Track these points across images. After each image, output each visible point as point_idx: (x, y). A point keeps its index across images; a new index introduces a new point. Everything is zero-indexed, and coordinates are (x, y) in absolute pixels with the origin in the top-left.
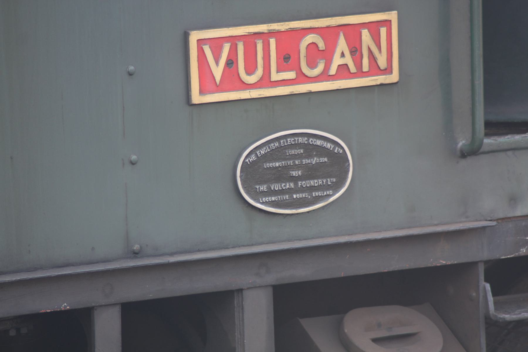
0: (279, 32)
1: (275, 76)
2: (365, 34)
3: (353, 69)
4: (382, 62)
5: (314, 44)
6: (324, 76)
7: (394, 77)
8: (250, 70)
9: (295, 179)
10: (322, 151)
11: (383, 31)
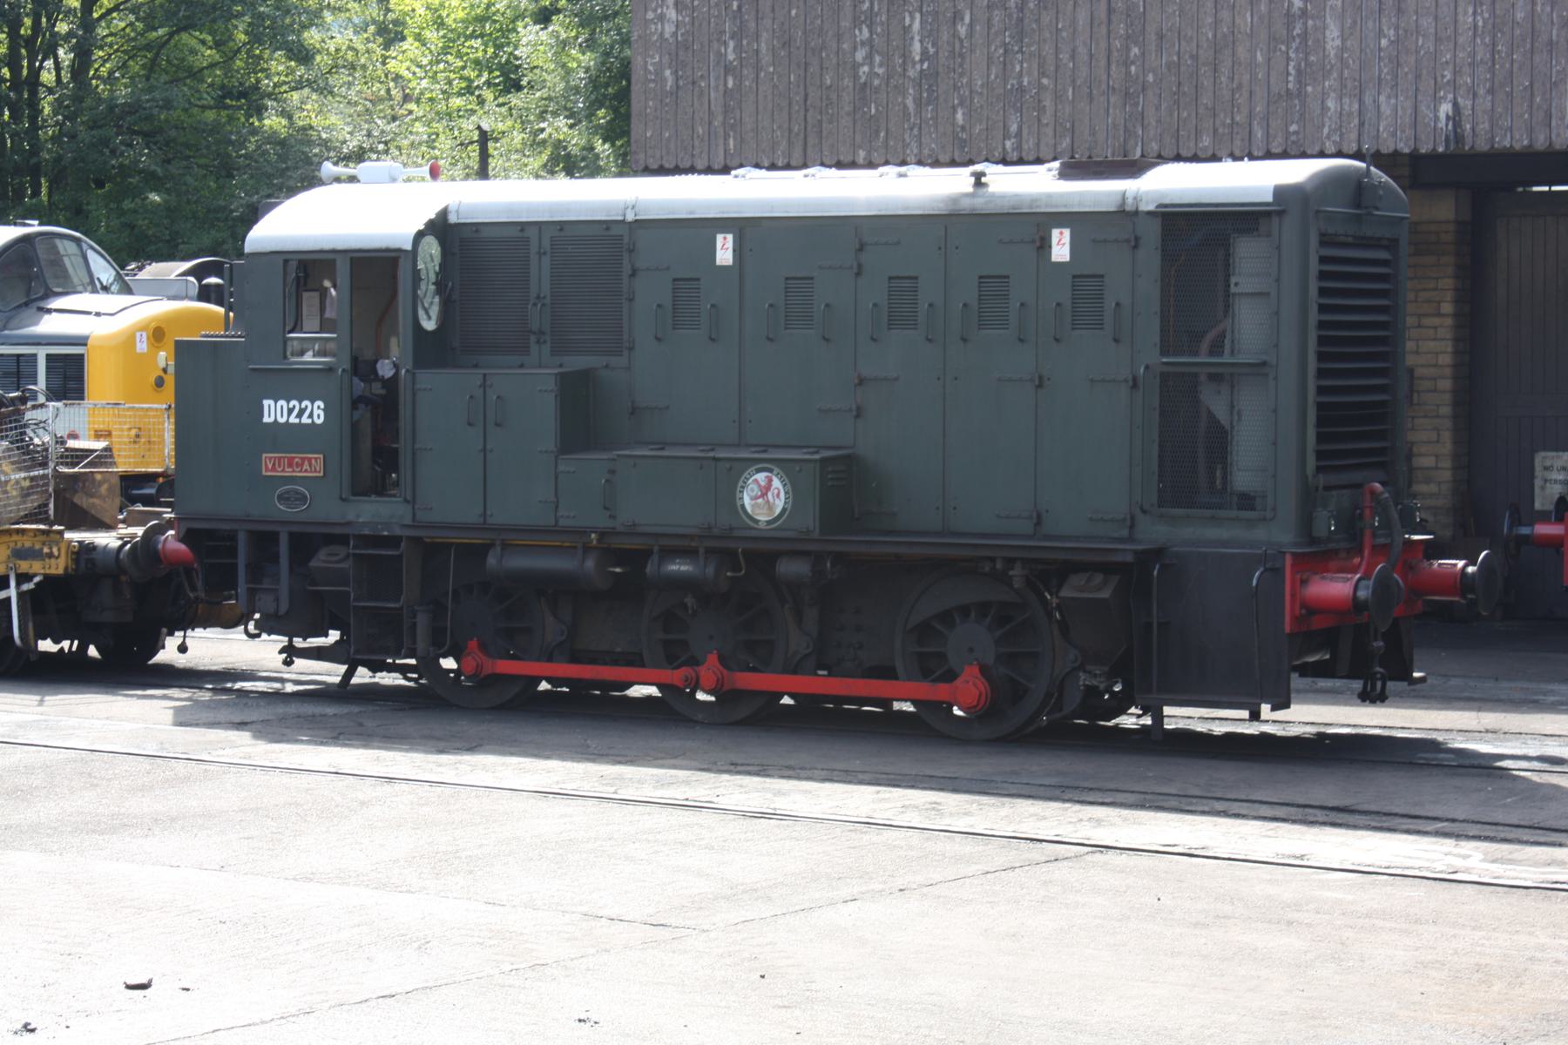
6: (301, 471)
8: (280, 466)
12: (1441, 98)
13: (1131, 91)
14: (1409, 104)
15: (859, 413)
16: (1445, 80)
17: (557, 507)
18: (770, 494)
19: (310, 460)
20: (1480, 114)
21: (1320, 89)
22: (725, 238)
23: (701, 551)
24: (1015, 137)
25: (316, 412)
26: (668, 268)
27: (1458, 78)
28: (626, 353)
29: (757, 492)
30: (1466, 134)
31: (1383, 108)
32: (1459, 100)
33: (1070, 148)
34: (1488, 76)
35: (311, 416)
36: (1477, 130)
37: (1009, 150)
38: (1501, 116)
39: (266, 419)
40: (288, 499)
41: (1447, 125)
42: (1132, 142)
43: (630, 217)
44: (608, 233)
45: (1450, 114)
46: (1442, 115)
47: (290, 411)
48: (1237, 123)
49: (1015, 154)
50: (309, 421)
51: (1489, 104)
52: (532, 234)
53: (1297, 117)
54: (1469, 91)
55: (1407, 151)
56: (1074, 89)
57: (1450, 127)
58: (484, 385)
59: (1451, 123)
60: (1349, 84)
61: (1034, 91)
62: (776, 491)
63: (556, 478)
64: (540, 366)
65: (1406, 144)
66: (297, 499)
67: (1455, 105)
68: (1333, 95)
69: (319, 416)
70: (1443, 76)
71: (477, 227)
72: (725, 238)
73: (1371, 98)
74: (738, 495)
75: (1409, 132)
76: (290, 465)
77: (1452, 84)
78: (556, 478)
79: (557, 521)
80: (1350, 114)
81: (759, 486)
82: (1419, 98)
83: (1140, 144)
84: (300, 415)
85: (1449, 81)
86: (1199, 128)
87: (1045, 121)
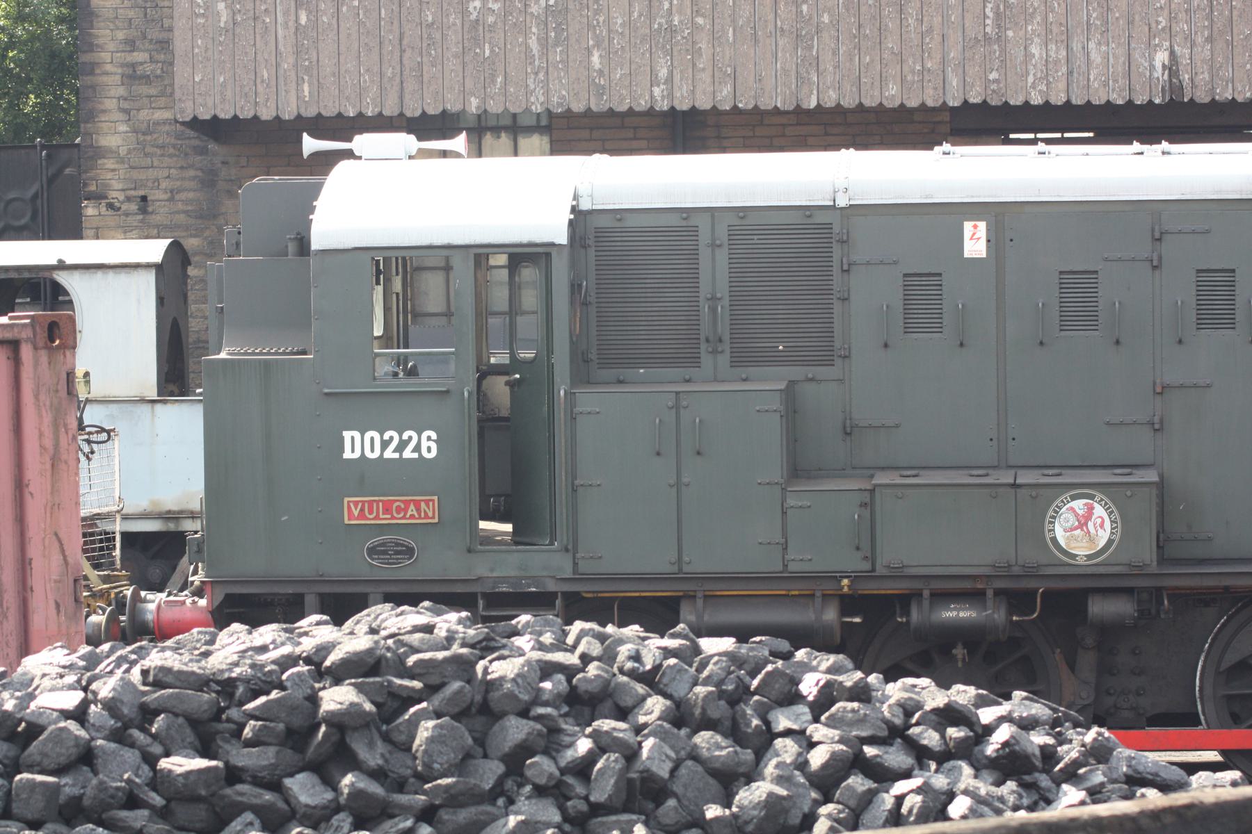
1: (381, 516)
3: (417, 516)
4: (430, 514)
5: (398, 507)
6: (404, 518)
7: (436, 520)
8: (371, 512)
10: (402, 545)
11: (431, 504)
12: (1156, 45)
13: (804, 33)
14: (1121, 52)
15: (1158, 428)
16: (1160, 27)
17: (785, 549)
18: (1090, 524)
20: (1199, 64)
21: (1022, 33)
22: (975, 227)
23: (990, 593)
24: (664, 84)
25: (428, 445)
26: (895, 263)
27: (1174, 25)
28: (838, 362)
29: (1073, 521)
30: (1184, 84)
31: (1093, 55)
32: (1176, 48)
33: (731, 96)
34: (1206, 24)
35: (417, 448)
36: (1197, 80)
37: (659, 99)
38: (1221, 67)
39: (348, 455)
40: (385, 553)
41: (1163, 74)
42: (805, 90)
43: (842, 202)
44: (744, 222)
45: (1166, 63)
46: (1158, 65)
47: (385, 445)
48: (929, 70)
49: (666, 102)
50: (416, 455)
51: (1209, 53)
52: (703, 223)
53: (997, 64)
54: (1186, 39)
55: (1120, 102)
56: (734, 30)
57: (1166, 77)
58: (677, 407)
59: (1167, 72)
60: (1055, 29)
61: (687, 32)
62: (1099, 520)
64: (716, 380)
65: (1119, 95)
67: (1172, 54)
68: (1036, 40)
69: (429, 450)
70: (1158, 23)
71: (619, 214)
72: (975, 227)
73: (1080, 46)
74: (1047, 527)
75: (1122, 82)
76: (387, 510)
77: (1168, 31)
78: (784, 513)
79: (785, 566)
80: (1057, 62)
81: (1076, 515)
82: (1133, 45)
83: (815, 92)
85: (1163, 29)
86: (884, 75)
87: (701, 66)
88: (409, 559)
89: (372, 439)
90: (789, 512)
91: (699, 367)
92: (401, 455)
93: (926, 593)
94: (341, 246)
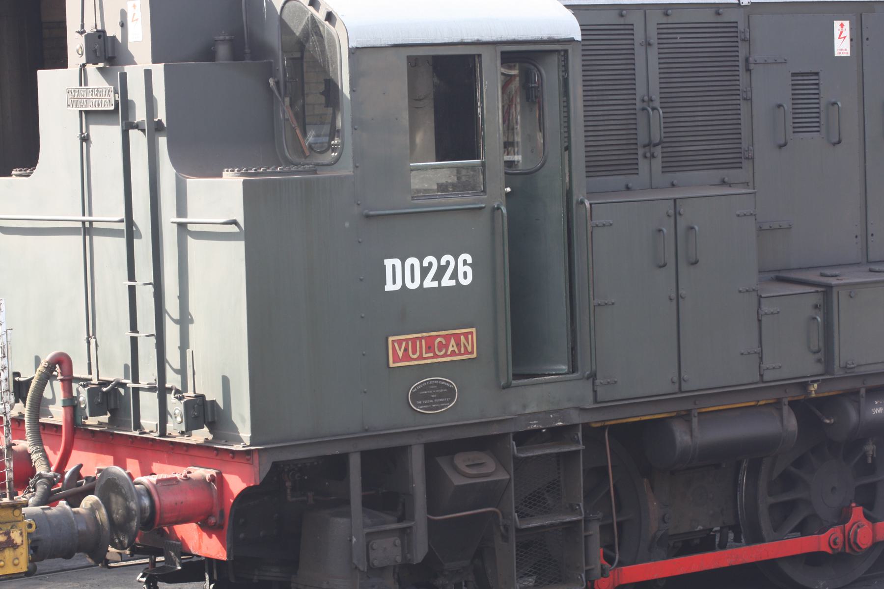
0: (426, 337)
1: (425, 355)
2: (462, 338)
3: (457, 352)
4: (469, 349)
5: (440, 342)
6: (445, 355)
7: (475, 355)
9: (433, 399)
10: (445, 387)
11: (470, 336)
17: (761, 358)
19: (457, 337)
22: (842, 26)
35: (454, 276)
39: (389, 287)
40: (427, 397)
47: (425, 271)
50: (453, 283)
52: (636, 19)
63: (760, 321)
66: (440, 396)
69: (465, 274)
72: (842, 26)
76: (430, 348)
78: (760, 321)
84: (438, 277)
88: (451, 402)
89: (412, 266)
90: (764, 320)
91: (637, 174)
92: (440, 284)
93: (863, 391)
94: (378, 43)
